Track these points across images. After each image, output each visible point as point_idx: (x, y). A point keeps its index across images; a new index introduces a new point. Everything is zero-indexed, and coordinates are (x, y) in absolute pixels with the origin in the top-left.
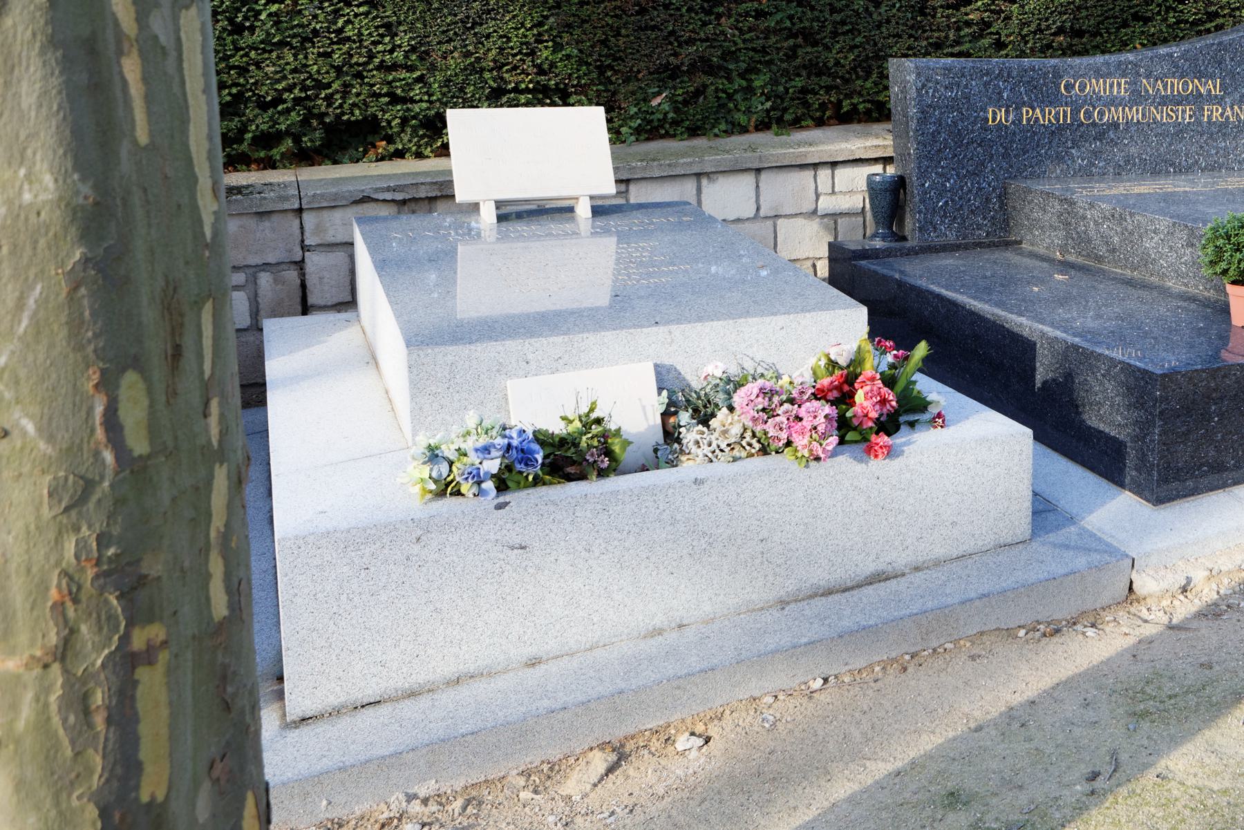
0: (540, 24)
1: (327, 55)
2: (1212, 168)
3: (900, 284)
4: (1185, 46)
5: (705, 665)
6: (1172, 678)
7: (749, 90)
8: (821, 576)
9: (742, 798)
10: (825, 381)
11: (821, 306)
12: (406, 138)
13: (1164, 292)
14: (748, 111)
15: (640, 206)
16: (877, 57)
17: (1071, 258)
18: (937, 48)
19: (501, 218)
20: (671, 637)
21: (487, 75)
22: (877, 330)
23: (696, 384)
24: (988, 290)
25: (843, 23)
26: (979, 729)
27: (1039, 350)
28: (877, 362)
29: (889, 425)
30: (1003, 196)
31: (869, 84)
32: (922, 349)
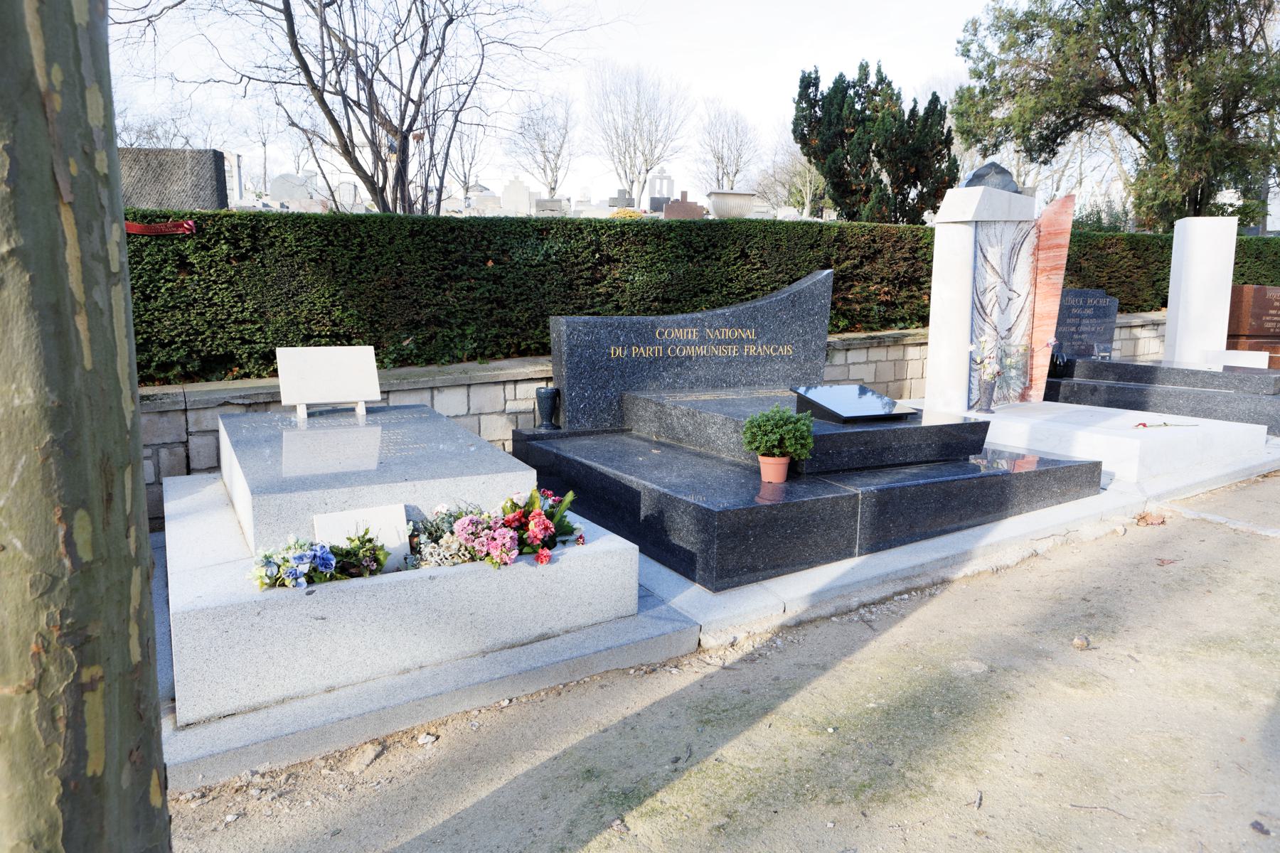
0: (334, 295)
1: (202, 314)
2: (750, 384)
3: (557, 456)
4: (733, 309)
5: (435, 691)
6: (725, 699)
7: (463, 336)
8: (508, 636)
9: (459, 774)
10: (511, 516)
11: (508, 469)
12: (251, 365)
13: (720, 461)
14: (463, 349)
15: (396, 408)
16: (543, 316)
17: (663, 440)
18: (579, 310)
19: (310, 415)
20: (416, 674)
21: (301, 327)
22: (543, 484)
23: (431, 518)
24: (611, 460)
25: (521, 294)
26: (605, 731)
27: (643, 497)
28: (543, 504)
29: (550, 543)
30: (620, 401)
31: (537, 332)
32: (570, 496)
